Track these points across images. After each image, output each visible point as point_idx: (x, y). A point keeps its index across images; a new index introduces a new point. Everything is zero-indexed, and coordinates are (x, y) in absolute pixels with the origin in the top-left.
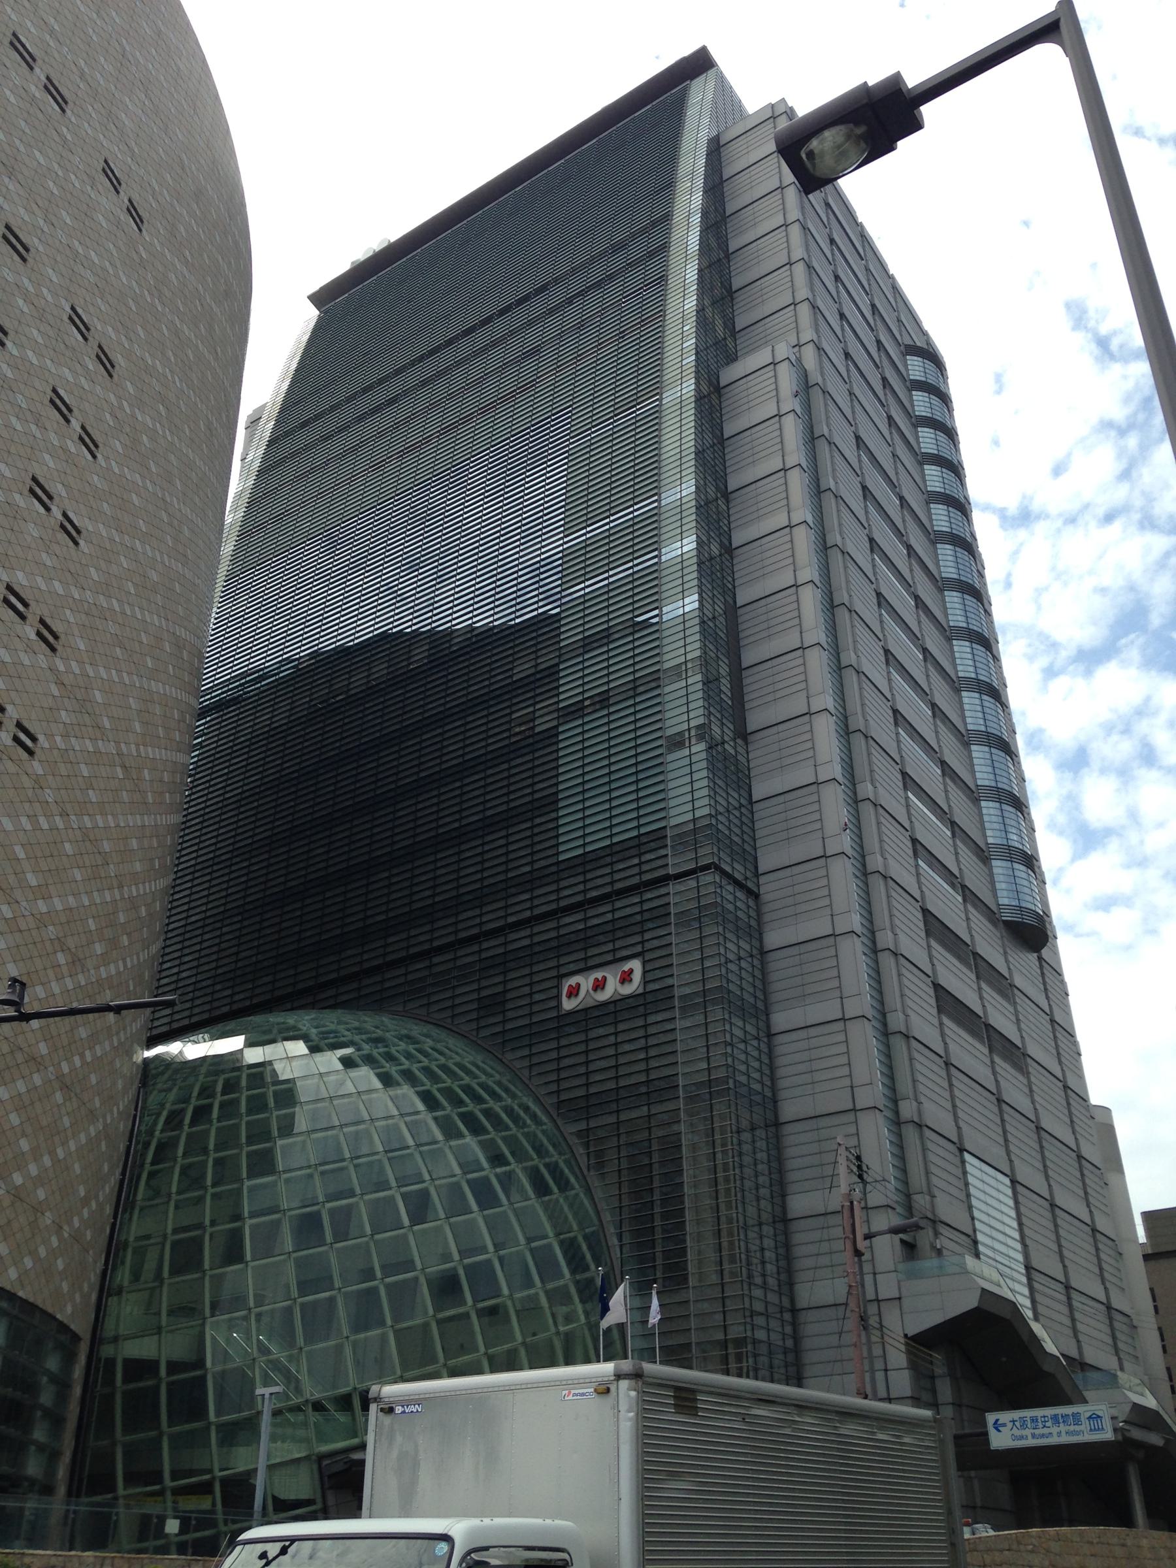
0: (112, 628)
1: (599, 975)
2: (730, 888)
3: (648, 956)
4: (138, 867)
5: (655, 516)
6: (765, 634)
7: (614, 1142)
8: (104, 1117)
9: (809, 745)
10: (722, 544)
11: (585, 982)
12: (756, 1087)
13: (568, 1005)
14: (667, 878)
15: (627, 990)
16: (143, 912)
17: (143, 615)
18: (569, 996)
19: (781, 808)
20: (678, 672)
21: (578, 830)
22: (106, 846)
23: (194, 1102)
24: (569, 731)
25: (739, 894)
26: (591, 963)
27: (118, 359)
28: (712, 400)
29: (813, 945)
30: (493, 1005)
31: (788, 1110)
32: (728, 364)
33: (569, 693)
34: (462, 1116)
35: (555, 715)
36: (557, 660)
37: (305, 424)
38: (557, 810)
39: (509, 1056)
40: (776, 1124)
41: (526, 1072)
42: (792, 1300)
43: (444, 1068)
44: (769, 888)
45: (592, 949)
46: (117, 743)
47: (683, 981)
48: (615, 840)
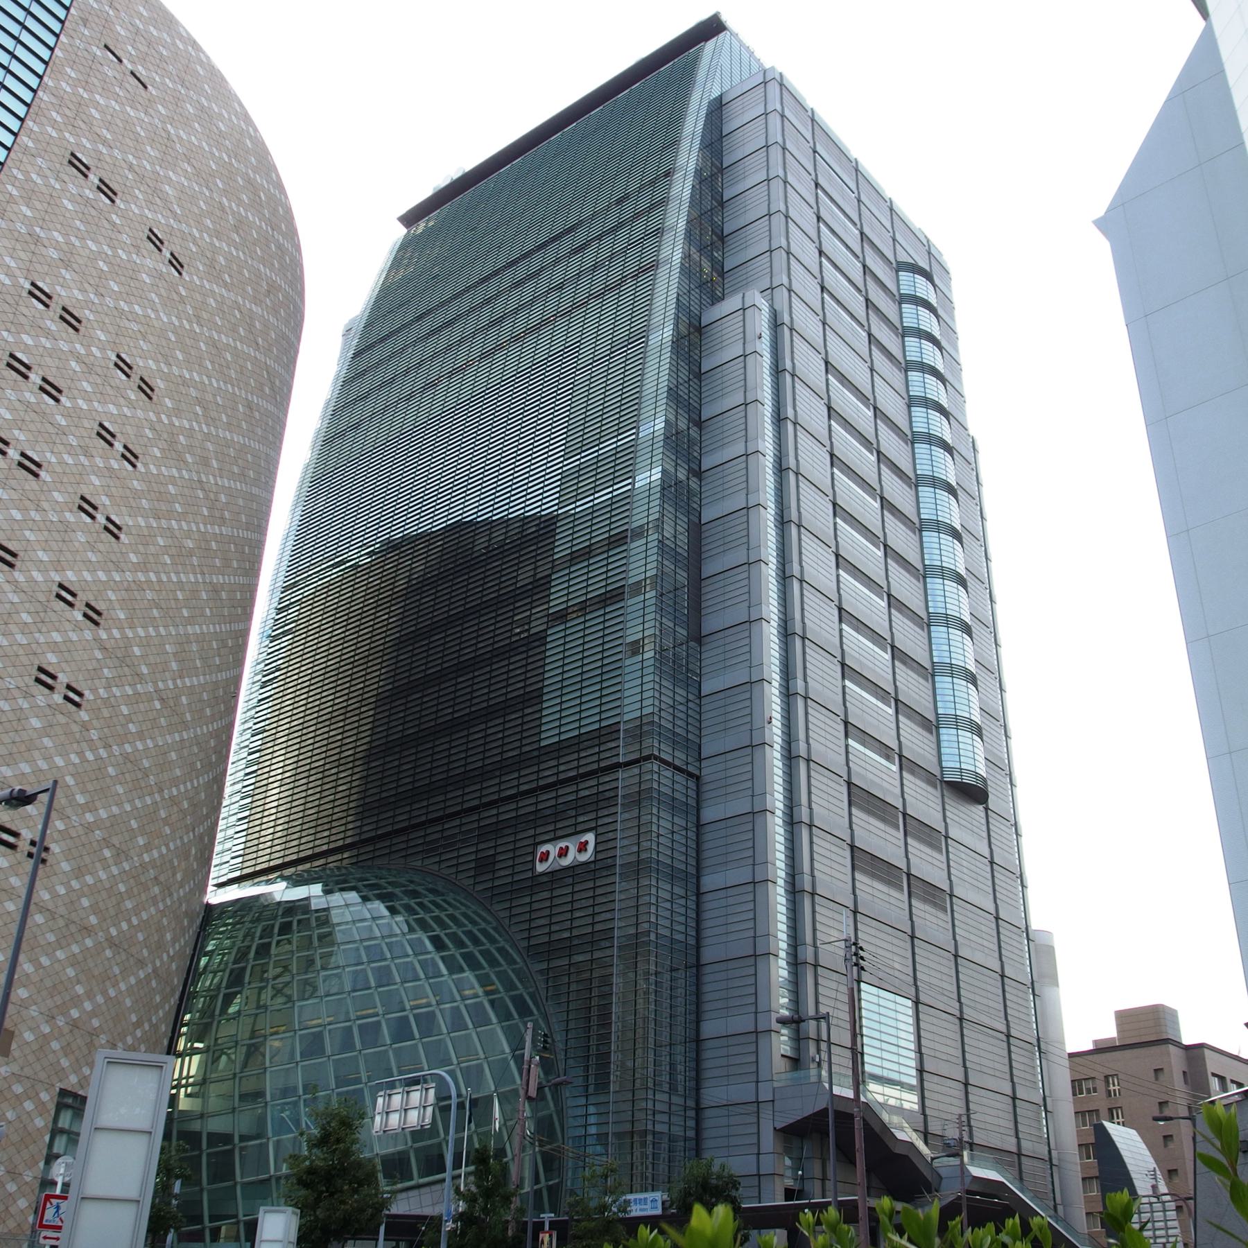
0: (149, 595)
1: (563, 844)
2: (668, 774)
3: (600, 830)
4: (178, 772)
5: (633, 446)
6: (721, 549)
7: (566, 979)
8: (153, 962)
9: (747, 649)
10: (690, 470)
11: (553, 849)
12: (681, 937)
13: (540, 868)
14: (618, 766)
15: (584, 857)
16: (186, 805)
17: (178, 577)
18: (541, 861)
19: (721, 703)
20: (638, 588)
21: (558, 720)
22: (146, 763)
23: (257, 941)
24: (555, 633)
25: (677, 778)
26: (560, 833)
27: (159, 384)
28: (693, 338)
29: (737, 821)
30: (485, 865)
31: (708, 955)
32: (713, 304)
33: (557, 601)
34: (464, 956)
35: (545, 619)
36: (549, 572)
37: (420, 318)
38: (542, 702)
39: (497, 907)
40: (699, 966)
41: (507, 921)
42: (698, 1102)
43: (452, 917)
44: (708, 771)
45: (560, 823)
46: (155, 683)
47: (623, 852)
48: (563, 737)
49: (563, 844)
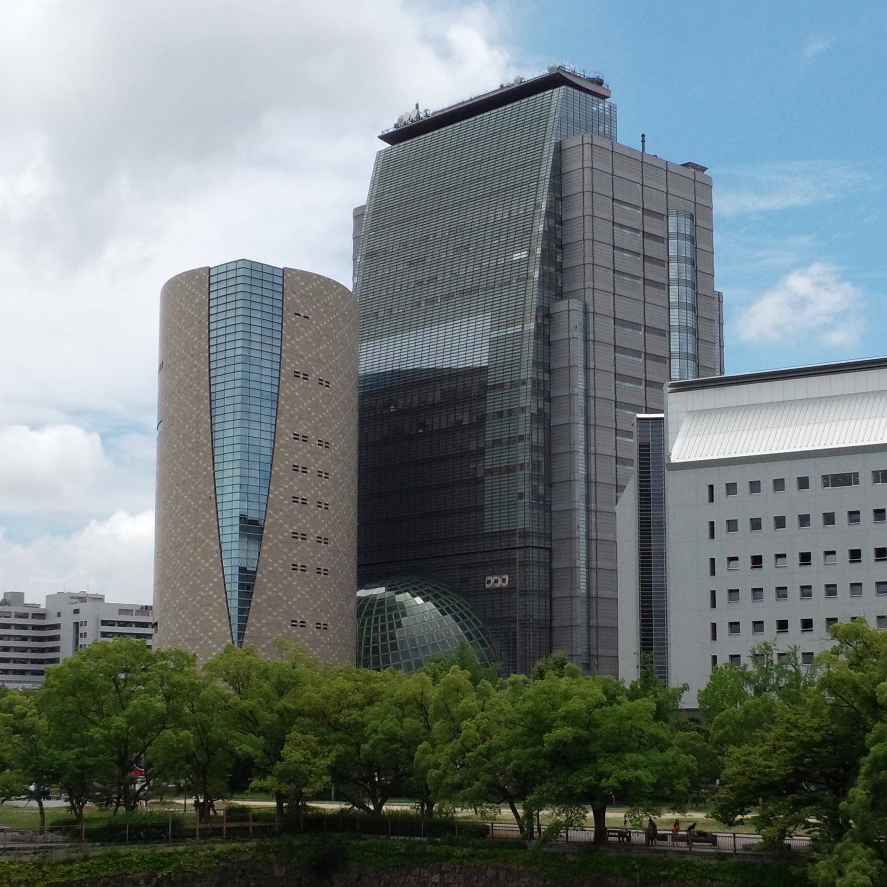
1: (496, 578)
11: (492, 579)
13: (487, 586)
21: (493, 522)
33: (488, 465)
40: (551, 628)
49: (496, 578)
